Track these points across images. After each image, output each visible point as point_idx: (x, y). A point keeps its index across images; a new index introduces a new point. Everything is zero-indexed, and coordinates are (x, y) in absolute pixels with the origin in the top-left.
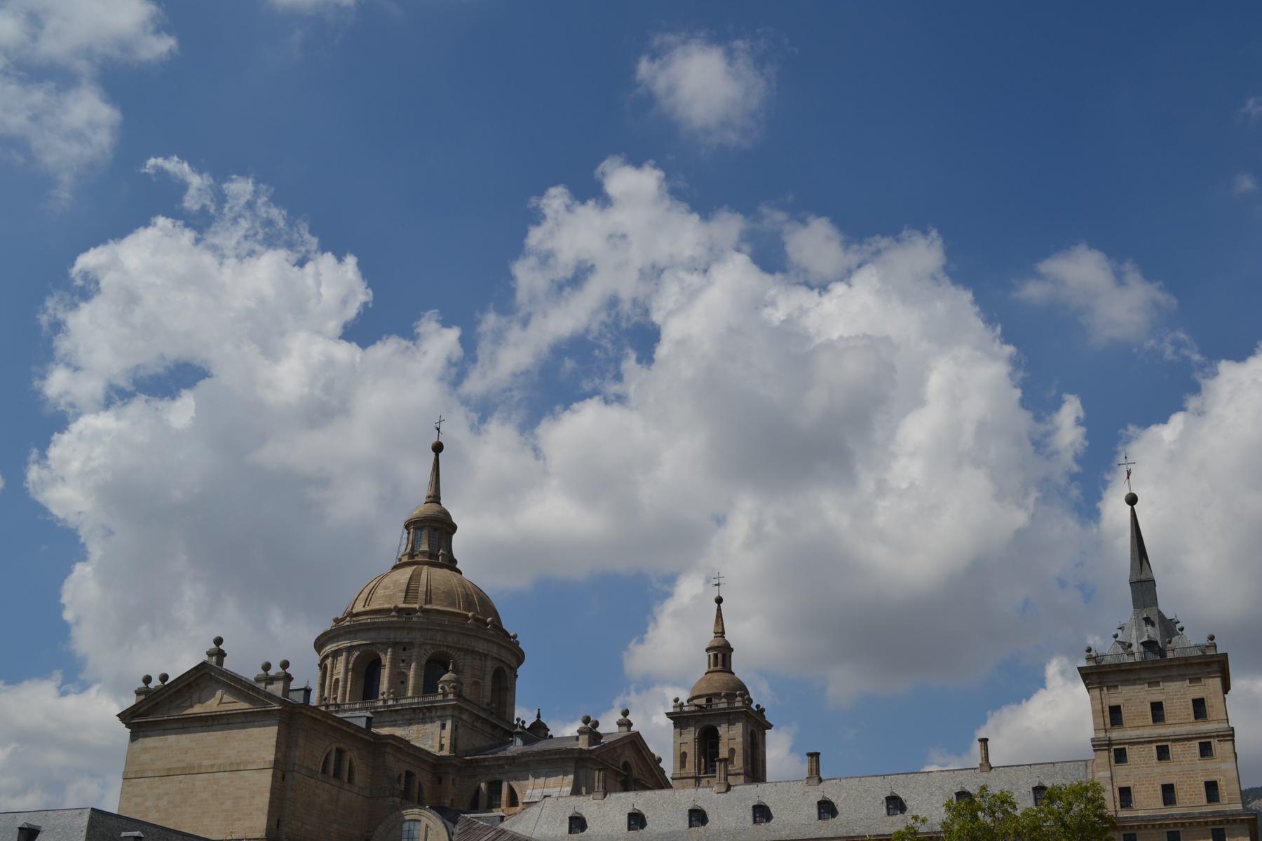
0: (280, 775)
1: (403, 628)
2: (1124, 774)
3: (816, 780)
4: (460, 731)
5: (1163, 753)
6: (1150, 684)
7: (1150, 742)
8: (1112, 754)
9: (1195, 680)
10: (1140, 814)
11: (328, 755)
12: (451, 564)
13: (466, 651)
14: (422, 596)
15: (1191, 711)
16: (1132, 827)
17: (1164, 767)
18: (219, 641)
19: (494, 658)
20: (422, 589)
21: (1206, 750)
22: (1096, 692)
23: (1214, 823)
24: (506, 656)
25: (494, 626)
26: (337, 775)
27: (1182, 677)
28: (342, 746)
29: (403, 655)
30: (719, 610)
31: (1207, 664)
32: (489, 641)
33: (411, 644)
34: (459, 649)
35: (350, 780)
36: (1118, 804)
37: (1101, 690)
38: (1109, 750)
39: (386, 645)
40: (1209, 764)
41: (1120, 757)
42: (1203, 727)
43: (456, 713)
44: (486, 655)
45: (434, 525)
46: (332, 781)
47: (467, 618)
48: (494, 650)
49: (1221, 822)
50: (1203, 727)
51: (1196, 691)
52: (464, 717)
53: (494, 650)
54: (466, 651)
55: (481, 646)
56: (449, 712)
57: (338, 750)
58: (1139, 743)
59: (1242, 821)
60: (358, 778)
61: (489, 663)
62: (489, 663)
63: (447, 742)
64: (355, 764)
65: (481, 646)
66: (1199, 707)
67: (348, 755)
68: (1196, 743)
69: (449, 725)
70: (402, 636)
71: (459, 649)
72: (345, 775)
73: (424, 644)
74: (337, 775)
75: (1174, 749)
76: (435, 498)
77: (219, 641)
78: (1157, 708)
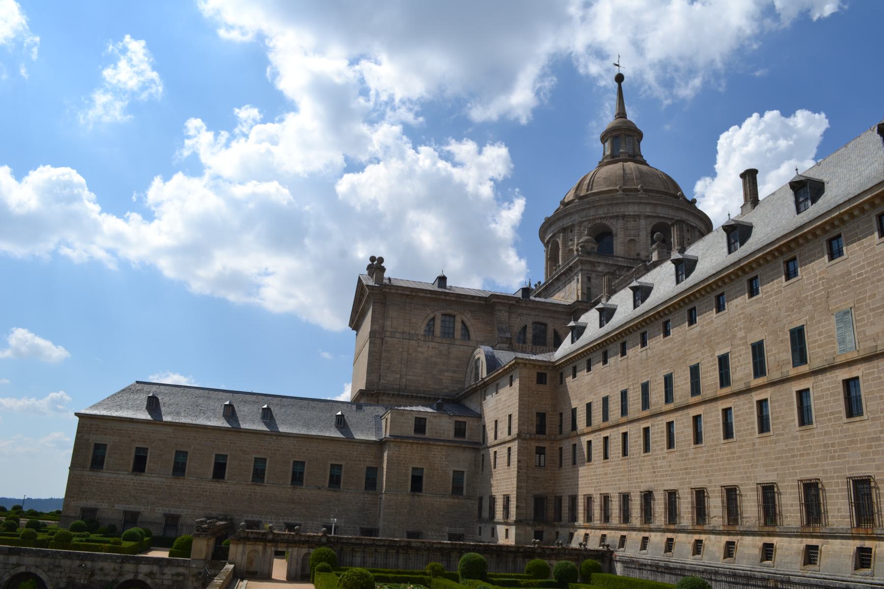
0: (378, 341)
1: (566, 216)
3: (749, 206)
4: (593, 281)
11: (433, 319)
12: (636, 157)
13: (617, 217)
14: (585, 187)
19: (649, 216)
20: (587, 182)
24: (661, 212)
25: (645, 191)
26: (448, 333)
28: (449, 311)
29: (570, 235)
32: (640, 203)
33: (573, 226)
34: (612, 217)
39: (559, 232)
43: (587, 267)
44: (639, 216)
45: (614, 134)
46: (440, 340)
47: (617, 191)
48: (648, 210)
52: (599, 269)
53: (648, 210)
54: (617, 217)
55: (632, 210)
56: (580, 268)
61: (643, 222)
62: (643, 222)
63: (580, 294)
64: (468, 324)
65: (632, 210)
67: (458, 319)
69: (580, 277)
70: (567, 222)
71: (612, 217)
72: (458, 334)
73: (583, 222)
74: (448, 333)
76: (621, 114)
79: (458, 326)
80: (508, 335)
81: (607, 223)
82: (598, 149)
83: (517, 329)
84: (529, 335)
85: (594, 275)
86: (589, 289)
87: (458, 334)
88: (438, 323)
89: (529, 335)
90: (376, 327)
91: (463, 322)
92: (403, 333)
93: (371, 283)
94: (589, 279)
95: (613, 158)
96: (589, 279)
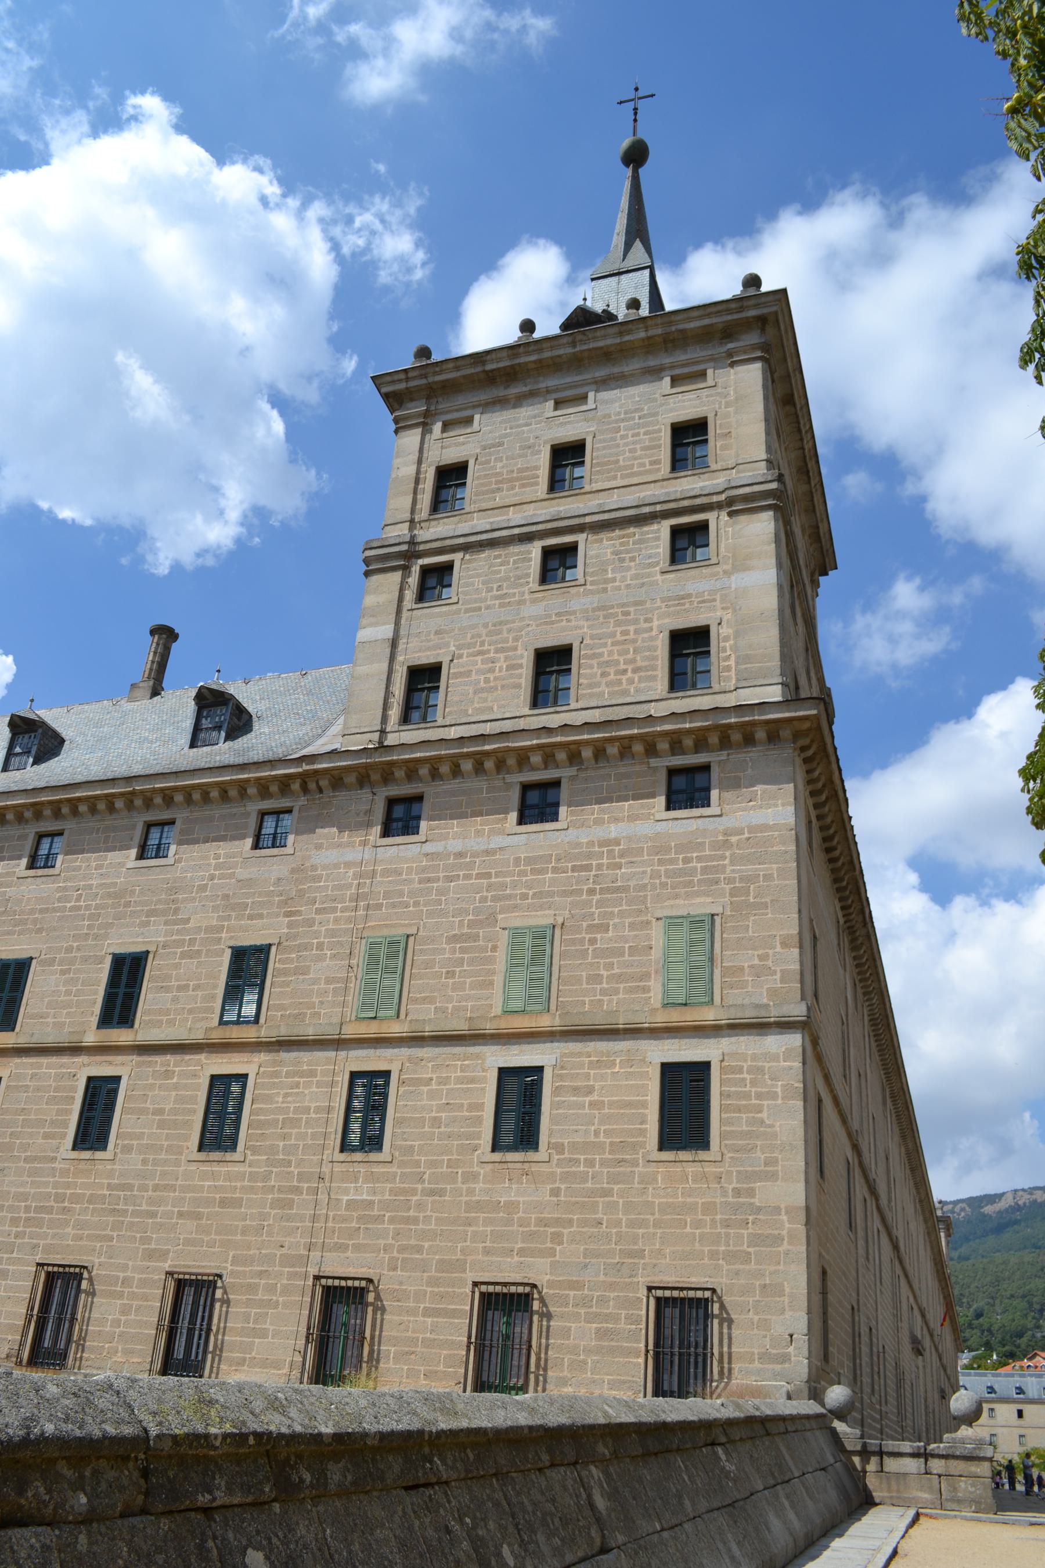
2: (430, 633)
5: (558, 561)
6: (558, 404)
7: (528, 538)
8: (414, 580)
9: (687, 377)
10: (453, 733)
15: (665, 454)
16: (412, 769)
17: (555, 598)
21: (688, 540)
22: (412, 439)
23: (676, 742)
27: (654, 373)
31: (728, 333)
36: (395, 713)
37: (426, 428)
38: (406, 569)
40: (693, 581)
41: (435, 580)
42: (690, 485)
49: (701, 743)
50: (690, 485)
51: (687, 405)
58: (492, 544)
59: (774, 732)
66: (689, 437)
68: (663, 529)
75: (592, 550)
78: (567, 455)
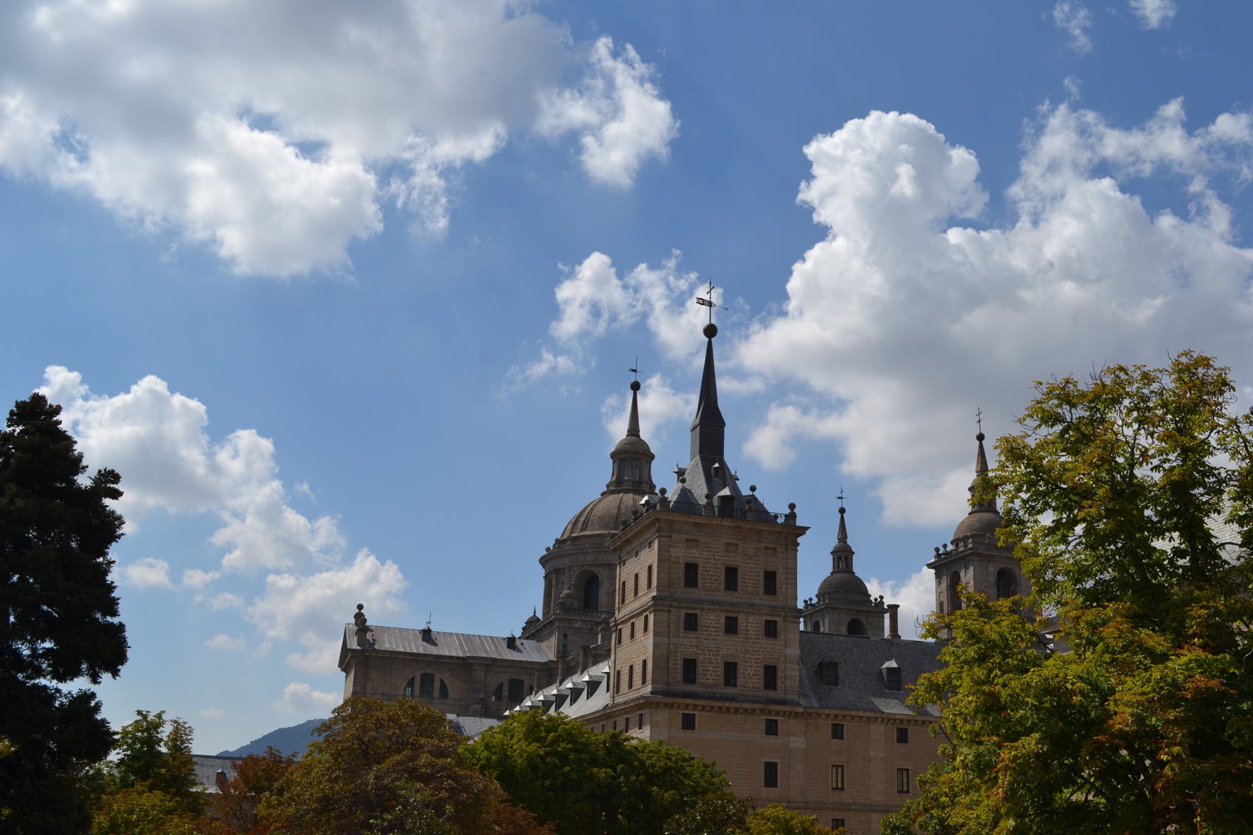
4: (569, 638)
11: (413, 679)
13: (603, 565)
14: (580, 525)
18: (360, 607)
20: (582, 519)
28: (428, 671)
30: (981, 447)
34: (599, 565)
35: (444, 693)
45: (622, 456)
54: (603, 565)
57: (423, 676)
60: (451, 695)
64: (447, 682)
67: (437, 678)
71: (599, 565)
72: (436, 693)
77: (360, 607)
79: (437, 685)
80: (482, 696)
81: (595, 570)
82: (605, 472)
83: (493, 687)
84: (505, 693)
85: (570, 632)
86: (565, 646)
87: (436, 693)
88: (417, 683)
89: (505, 693)
90: (358, 688)
91: (442, 681)
92: (383, 694)
93: (354, 644)
94: (565, 636)
95: (617, 486)
96: (565, 636)
